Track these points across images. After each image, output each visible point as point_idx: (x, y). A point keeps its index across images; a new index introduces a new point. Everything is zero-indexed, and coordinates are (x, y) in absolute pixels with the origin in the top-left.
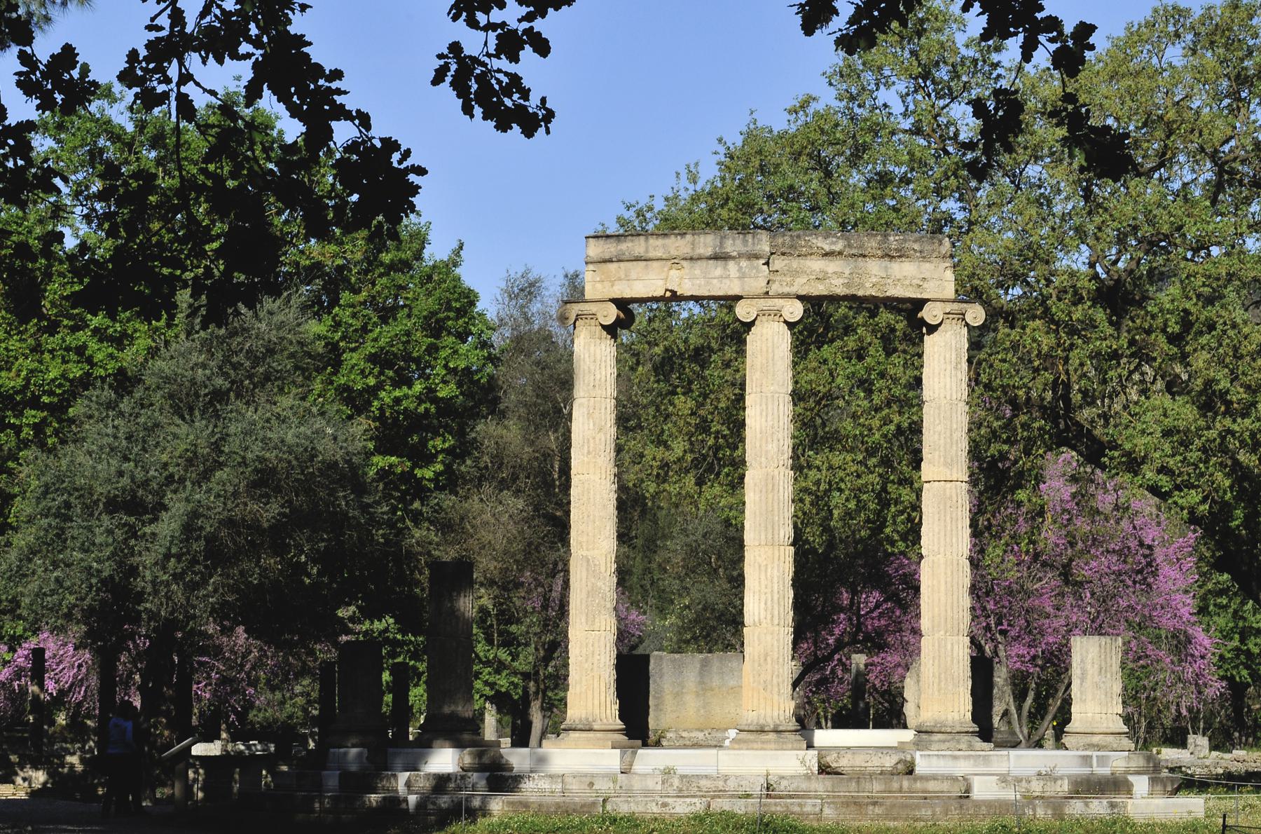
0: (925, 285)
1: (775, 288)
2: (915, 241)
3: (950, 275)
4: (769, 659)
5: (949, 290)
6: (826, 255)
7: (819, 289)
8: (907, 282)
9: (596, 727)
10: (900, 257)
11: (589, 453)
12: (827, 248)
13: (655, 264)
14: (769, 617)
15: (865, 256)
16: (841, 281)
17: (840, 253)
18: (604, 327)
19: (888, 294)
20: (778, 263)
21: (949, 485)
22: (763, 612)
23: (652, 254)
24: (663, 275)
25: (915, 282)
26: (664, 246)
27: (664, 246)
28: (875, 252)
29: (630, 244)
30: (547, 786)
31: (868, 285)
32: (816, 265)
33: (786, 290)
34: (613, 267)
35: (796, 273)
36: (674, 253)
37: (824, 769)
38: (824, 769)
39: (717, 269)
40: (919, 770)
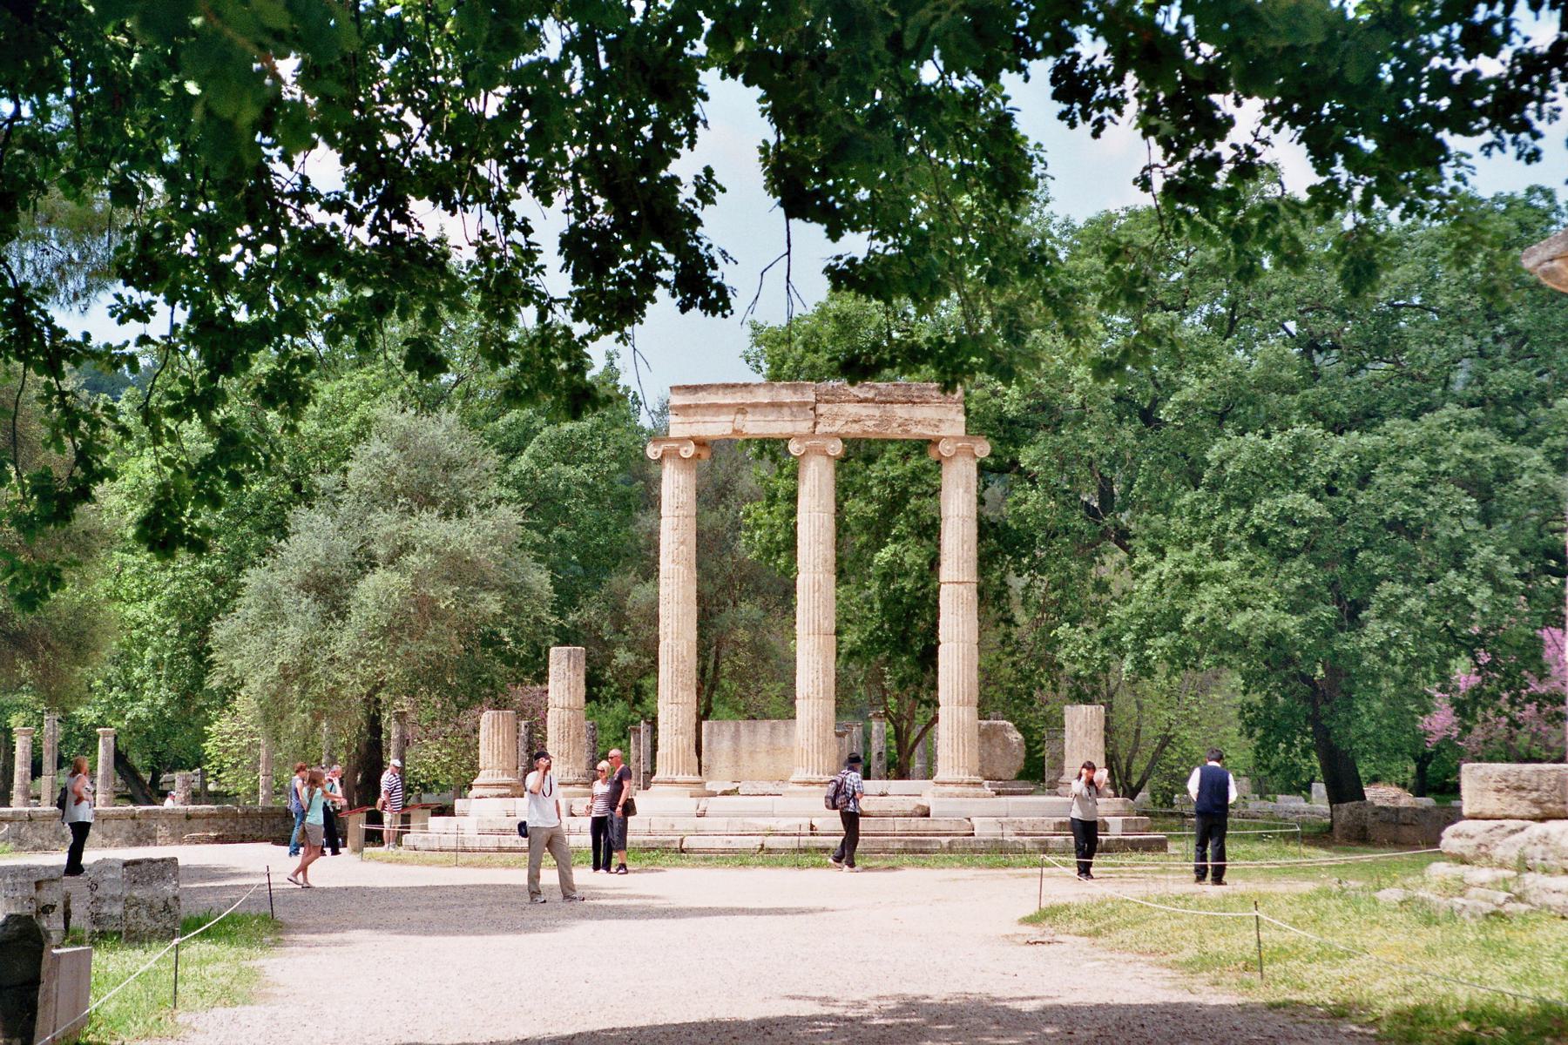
5: (960, 430)
7: (855, 430)
20: (822, 408)
32: (852, 409)
33: (829, 429)
35: (835, 417)
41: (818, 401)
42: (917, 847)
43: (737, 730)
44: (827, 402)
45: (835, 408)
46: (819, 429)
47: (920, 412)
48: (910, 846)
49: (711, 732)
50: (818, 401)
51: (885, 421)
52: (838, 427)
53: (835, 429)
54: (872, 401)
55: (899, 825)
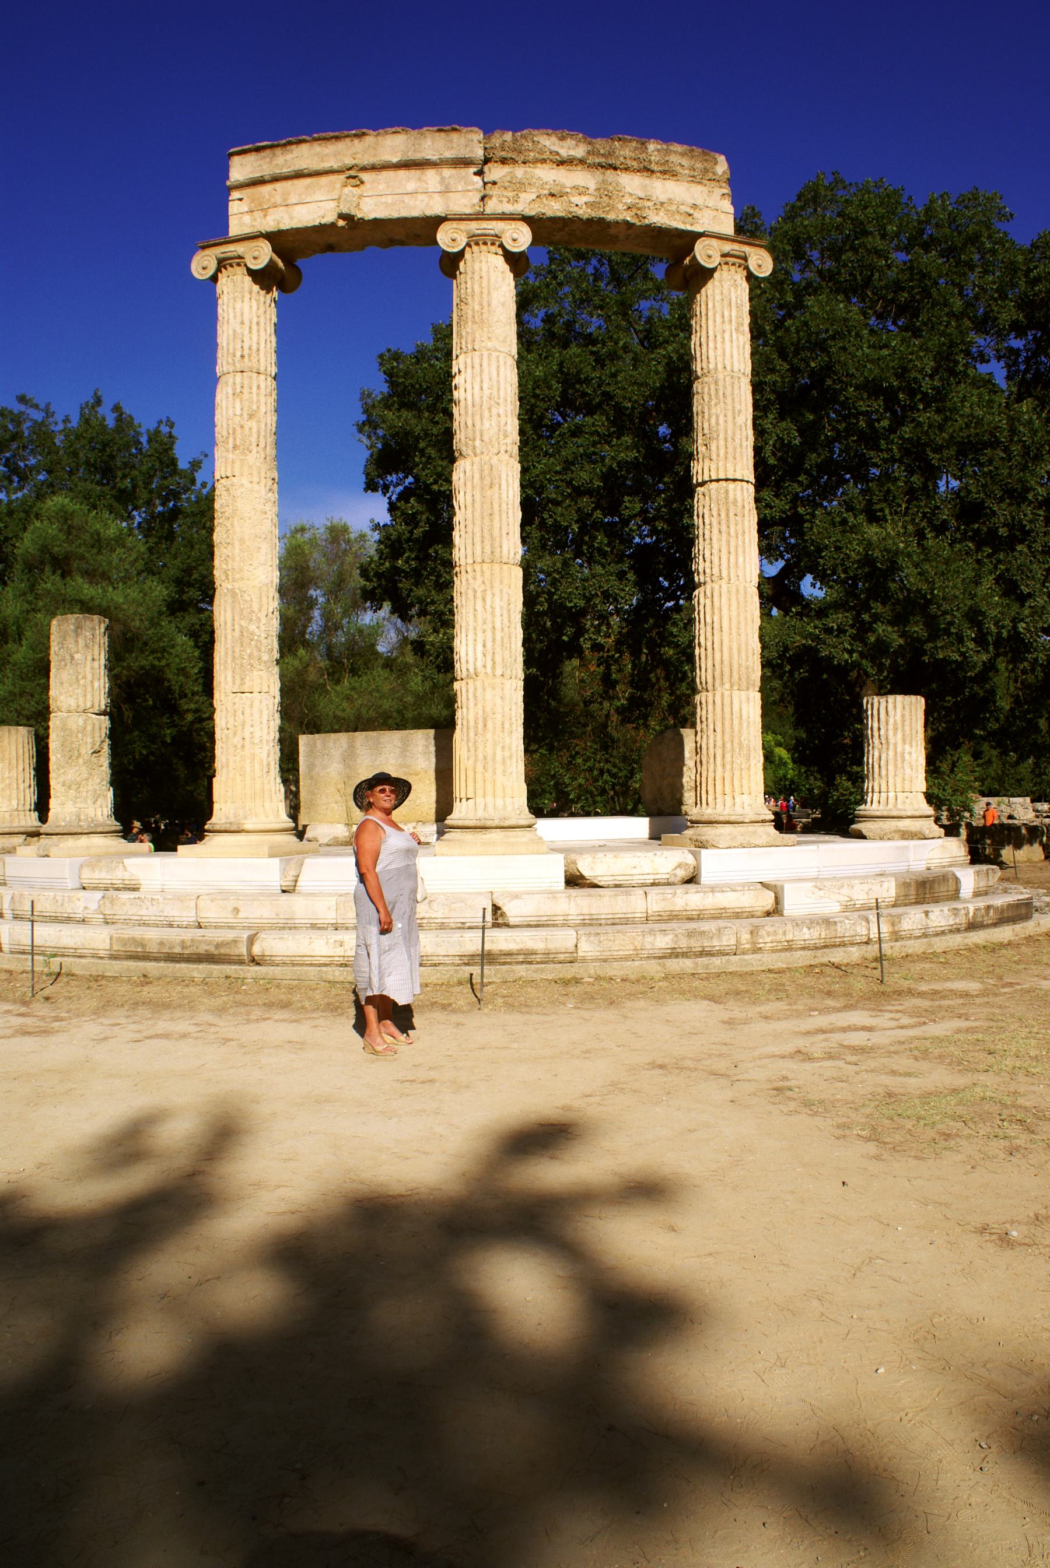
0: (696, 215)
1: (493, 206)
2: (683, 155)
3: (727, 206)
4: (490, 725)
5: (728, 227)
6: (561, 163)
7: (555, 209)
8: (674, 208)
9: (248, 826)
10: (664, 172)
11: (235, 447)
12: (564, 153)
13: (324, 180)
14: (489, 665)
15: (615, 169)
16: (585, 199)
17: (582, 161)
18: (251, 273)
19: (647, 222)
20: (495, 172)
21: (731, 486)
22: (480, 656)
25: (683, 209)
28: (629, 162)
31: (620, 206)
32: (548, 175)
33: (508, 208)
35: (521, 186)
36: (349, 161)
37: (574, 881)
38: (574, 881)
39: (408, 180)
40: (705, 878)
41: (487, 161)
42: (696, 944)
43: (351, 746)
44: (504, 161)
45: (520, 172)
47: (663, 189)
48: (683, 944)
49: (311, 752)
50: (487, 161)
51: (605, 192)
52: (526, 204)
53: (519, 208)
54: (582, 161)
55: (657, 902)
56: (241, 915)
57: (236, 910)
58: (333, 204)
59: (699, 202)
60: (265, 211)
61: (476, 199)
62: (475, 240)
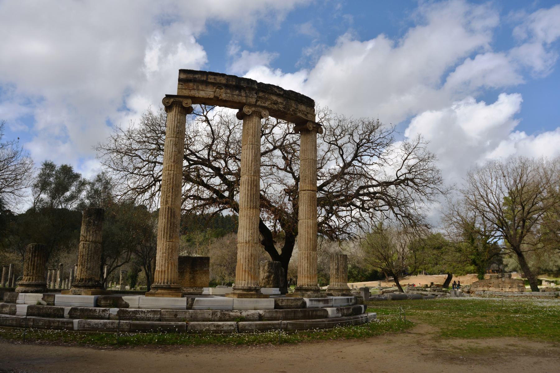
20: (261, 94)
23: (209, 80)
24: (214, 90)
26: (214, 78)
27: (214, 78)
29: (200, 76)
30: (151, 316)
32: (274, 98)
33: (263, 105)
34: (191, 84)
35: (267, 99)
46: (259, 103)
53: (266, 105)
56: (178, 317)
57: (176, 315)
58: (212, 93)
59: (308, 111)
60: (190, 90)
61: (255, 101)
62: (254, 113)
